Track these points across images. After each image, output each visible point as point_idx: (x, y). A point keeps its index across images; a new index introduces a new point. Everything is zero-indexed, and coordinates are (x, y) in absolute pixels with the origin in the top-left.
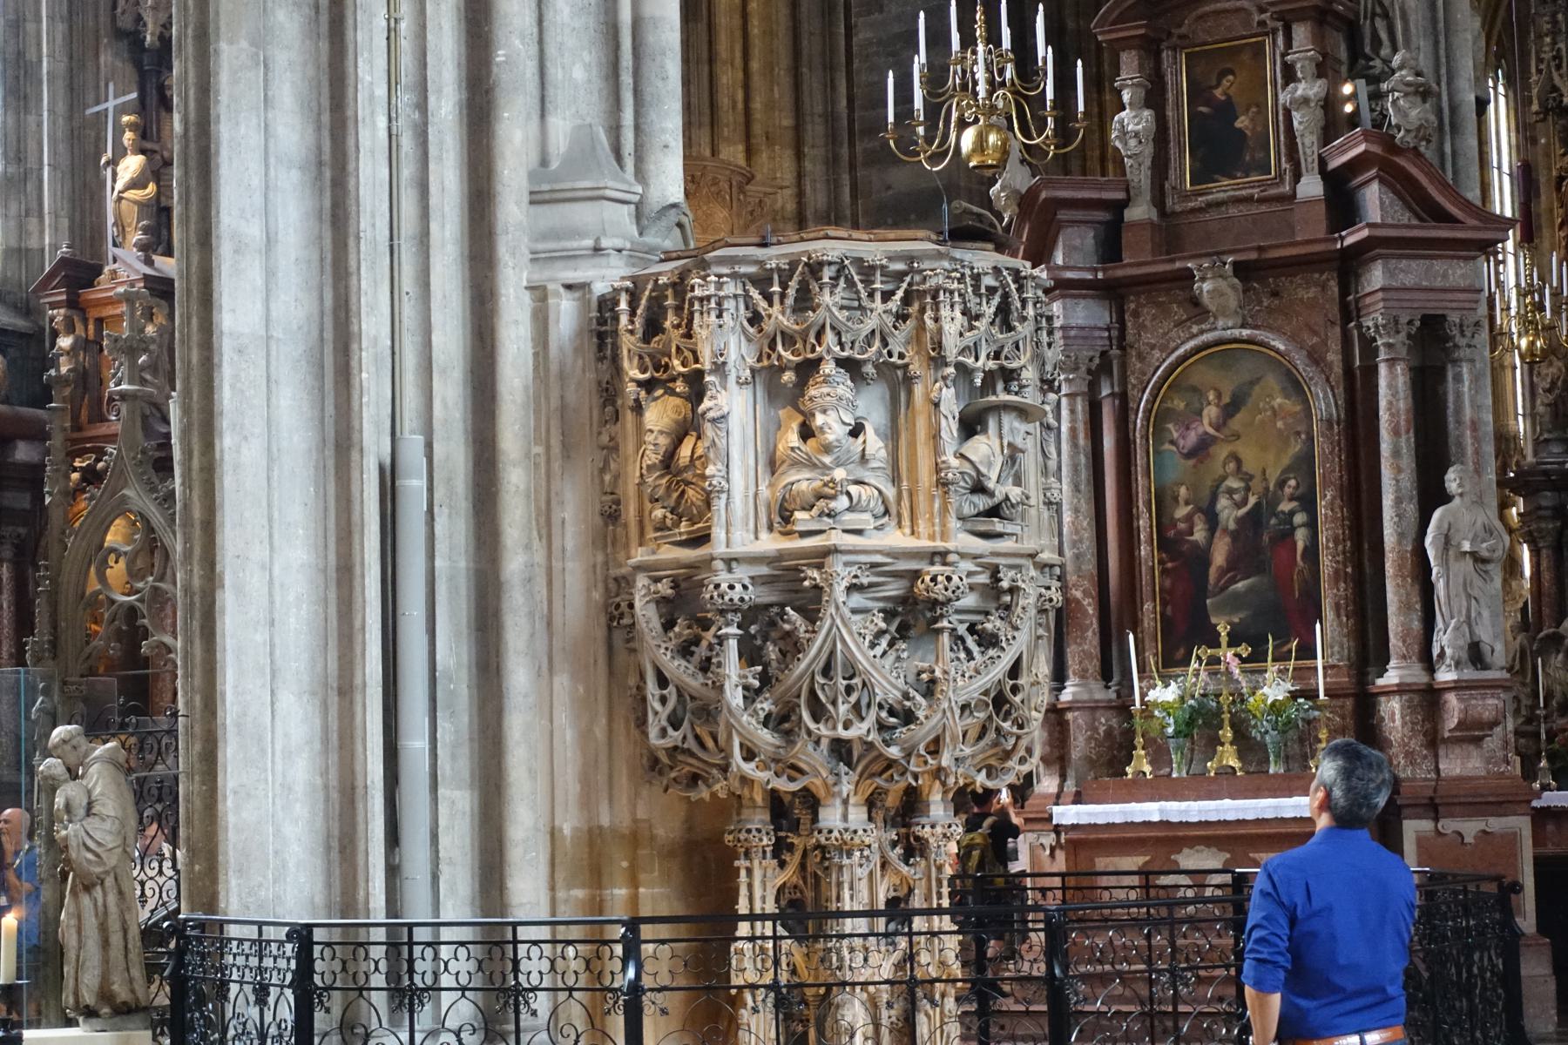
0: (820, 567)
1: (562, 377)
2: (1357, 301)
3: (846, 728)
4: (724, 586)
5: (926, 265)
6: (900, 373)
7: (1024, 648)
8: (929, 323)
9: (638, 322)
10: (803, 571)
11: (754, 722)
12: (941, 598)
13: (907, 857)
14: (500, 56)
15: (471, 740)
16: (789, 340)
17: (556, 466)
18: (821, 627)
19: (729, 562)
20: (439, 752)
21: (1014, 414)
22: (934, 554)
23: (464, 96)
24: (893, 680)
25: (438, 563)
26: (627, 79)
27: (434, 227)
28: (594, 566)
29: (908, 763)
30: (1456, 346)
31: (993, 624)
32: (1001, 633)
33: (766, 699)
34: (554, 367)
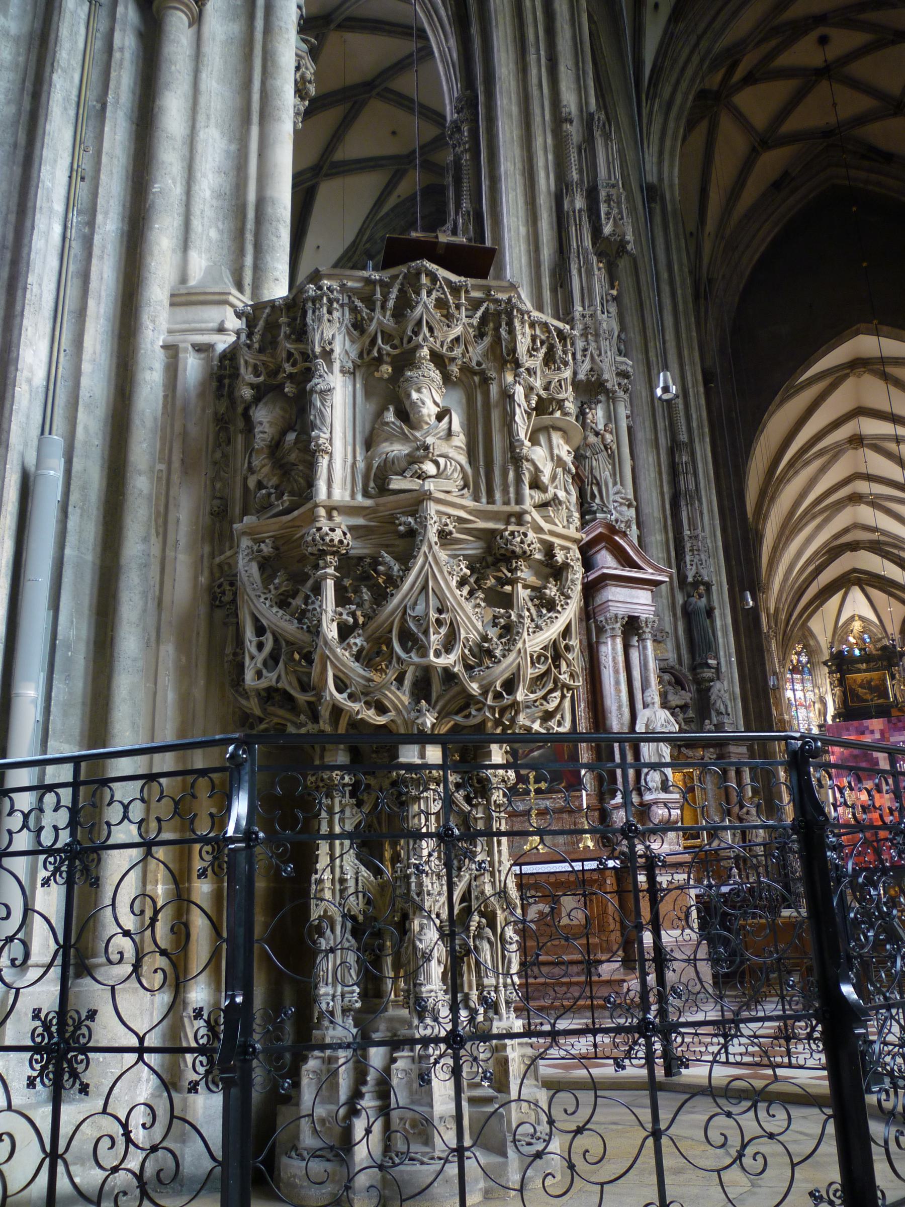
0: (413, 514)
1: (184, 409)
2: (594, 609)
3: (438, 654)
4: (326, 529)
6: (476, 379)
7: (572, 615)
8: (503, 332)
9: (256, 338)
10: (398, 519)
11: (347, 654)
12: (518, 550)
13: (468, 799)
14: (156, 187)
15: (84, 704)
16: (388, 337)
17: (175, 477)
18: (414, 564)
19: (330, 510)
20: (53, 708)
21: (559, 433)
22: (510, 515)
23: (126, 228)
24: (475, 621)
25: (68, 551)
26: (249, 237)
27: (91, 303)
28: (202, 556)
29: (486, 699)
30: (644, 632)
31: (552, 591)
32: (557, 598)
33: (359, 635)
34: (179, 403)
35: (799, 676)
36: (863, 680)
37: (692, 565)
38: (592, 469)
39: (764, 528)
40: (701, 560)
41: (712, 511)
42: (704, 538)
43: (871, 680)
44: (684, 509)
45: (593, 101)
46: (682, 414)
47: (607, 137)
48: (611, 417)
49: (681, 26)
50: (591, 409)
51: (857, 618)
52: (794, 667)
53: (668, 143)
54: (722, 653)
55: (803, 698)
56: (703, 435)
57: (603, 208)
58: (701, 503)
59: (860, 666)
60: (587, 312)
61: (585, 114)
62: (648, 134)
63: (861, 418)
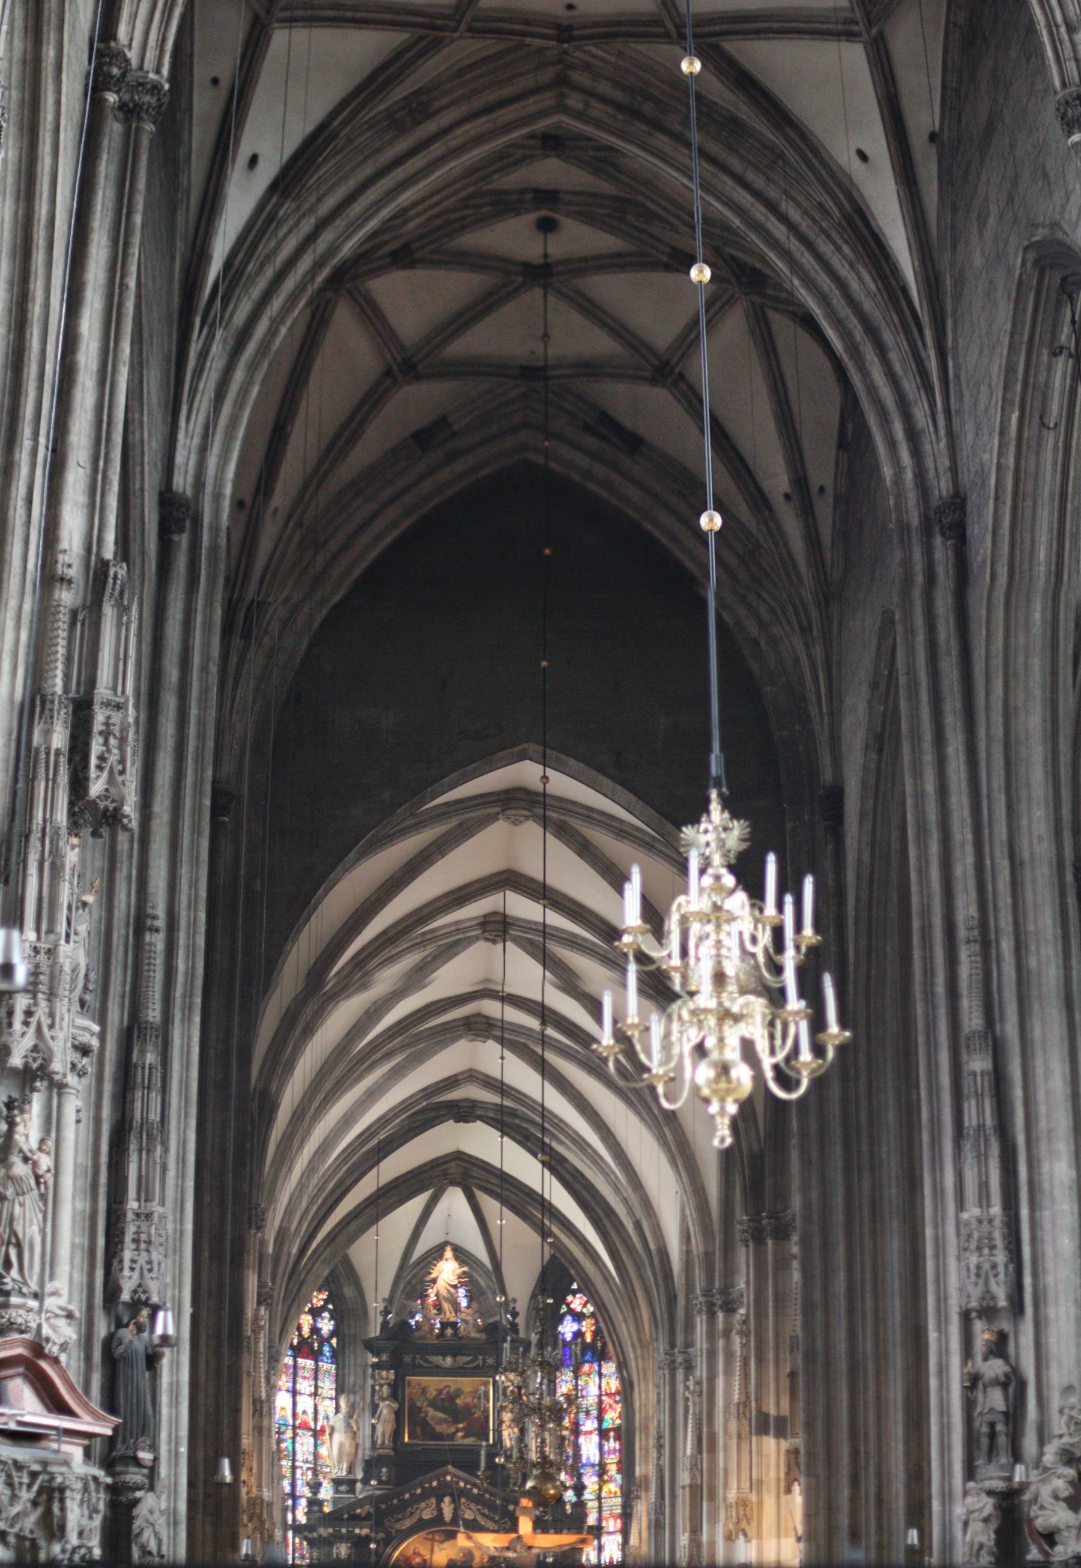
5: (52, 1469)
35: (309, 1363)
36: (440, 1392)
37: (132, 1269)
38: (11, 1219)
39: (280, 1091)
40: (150, 1262)
41: (184, 1162)
42: (163, 1217)
43: (459, 1393)
44: (134, 1157)
45: (110, 536)
46: (159, 961)
47: (123, 610)
48: (51, 1122)
49: (289, 206)
50: (22, 1112)
51: (449, 1253)
52: (302, 1341)
53: (227, 409)
54: (164, 1435)
55: (310, 1411)
56: (188, 1008)
57: (96, 747)
58: (166, 1150)
59: (437, 1359)
60: (43, 945)
61: (93, 558)
62: (193, 392)
63: (508, 892)
